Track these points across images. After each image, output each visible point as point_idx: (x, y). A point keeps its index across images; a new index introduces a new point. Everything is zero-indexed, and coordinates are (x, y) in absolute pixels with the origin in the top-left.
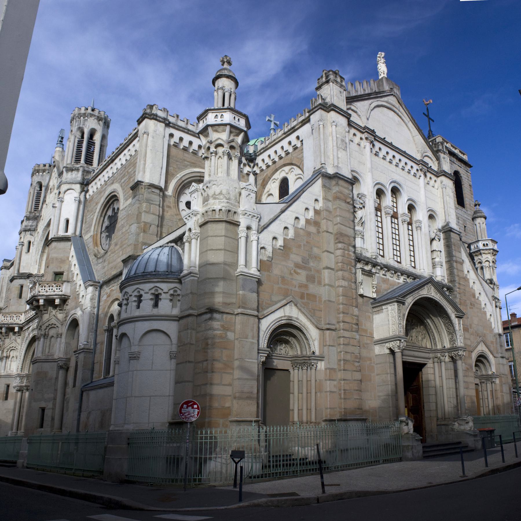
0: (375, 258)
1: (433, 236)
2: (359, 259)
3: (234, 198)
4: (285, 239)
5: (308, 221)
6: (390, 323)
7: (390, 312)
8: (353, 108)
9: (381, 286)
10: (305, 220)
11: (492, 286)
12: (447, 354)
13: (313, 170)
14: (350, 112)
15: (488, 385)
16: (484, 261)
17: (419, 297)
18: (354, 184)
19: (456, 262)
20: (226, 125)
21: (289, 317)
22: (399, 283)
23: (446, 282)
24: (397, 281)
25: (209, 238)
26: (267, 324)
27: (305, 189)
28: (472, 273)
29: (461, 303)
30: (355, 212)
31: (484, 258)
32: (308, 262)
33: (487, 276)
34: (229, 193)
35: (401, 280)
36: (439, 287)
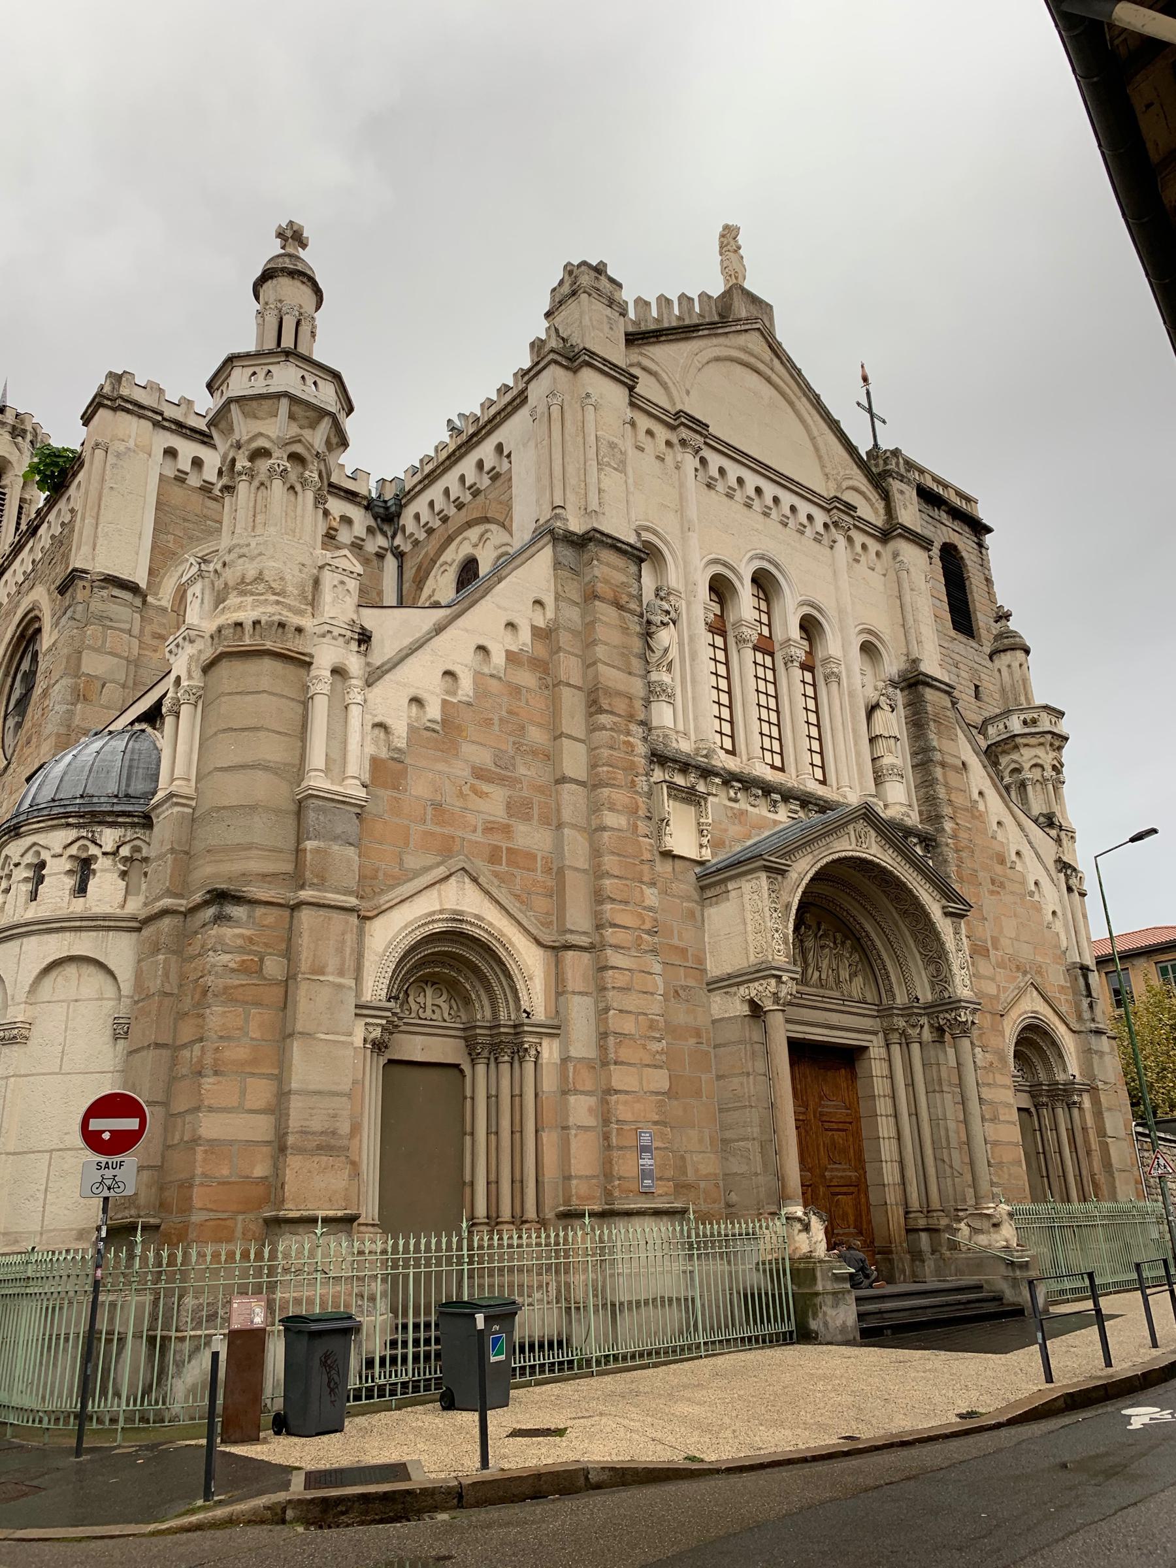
0: (706, 756)
1: (873, 696)
2: (659, 758)
3: (296, 592)
4: (445, 702)
5: (511, 657)
6: (749, 928)
7: (747, 897)
8: (646, 362)
9: (726, 830)
11: (1053, 833)
12: (924, 1020)
14: (635, 371)
15: (1060, 1111)
16: (1027, 766)
17: (830, 858)
18: (642, 561)
19: (943, 765)
20: (278, 396)
21: (455, 912)
22: (775, 822)
23: (913, 819)
24: (771, 816)
25: (224, 699)
26: (391, 933)
28: (992, 796)
31: (1026, 756)
32: (514, 765)
33: (1037, 808)
34: (282, 579)
35: (782, 815)
36: (893, 833)
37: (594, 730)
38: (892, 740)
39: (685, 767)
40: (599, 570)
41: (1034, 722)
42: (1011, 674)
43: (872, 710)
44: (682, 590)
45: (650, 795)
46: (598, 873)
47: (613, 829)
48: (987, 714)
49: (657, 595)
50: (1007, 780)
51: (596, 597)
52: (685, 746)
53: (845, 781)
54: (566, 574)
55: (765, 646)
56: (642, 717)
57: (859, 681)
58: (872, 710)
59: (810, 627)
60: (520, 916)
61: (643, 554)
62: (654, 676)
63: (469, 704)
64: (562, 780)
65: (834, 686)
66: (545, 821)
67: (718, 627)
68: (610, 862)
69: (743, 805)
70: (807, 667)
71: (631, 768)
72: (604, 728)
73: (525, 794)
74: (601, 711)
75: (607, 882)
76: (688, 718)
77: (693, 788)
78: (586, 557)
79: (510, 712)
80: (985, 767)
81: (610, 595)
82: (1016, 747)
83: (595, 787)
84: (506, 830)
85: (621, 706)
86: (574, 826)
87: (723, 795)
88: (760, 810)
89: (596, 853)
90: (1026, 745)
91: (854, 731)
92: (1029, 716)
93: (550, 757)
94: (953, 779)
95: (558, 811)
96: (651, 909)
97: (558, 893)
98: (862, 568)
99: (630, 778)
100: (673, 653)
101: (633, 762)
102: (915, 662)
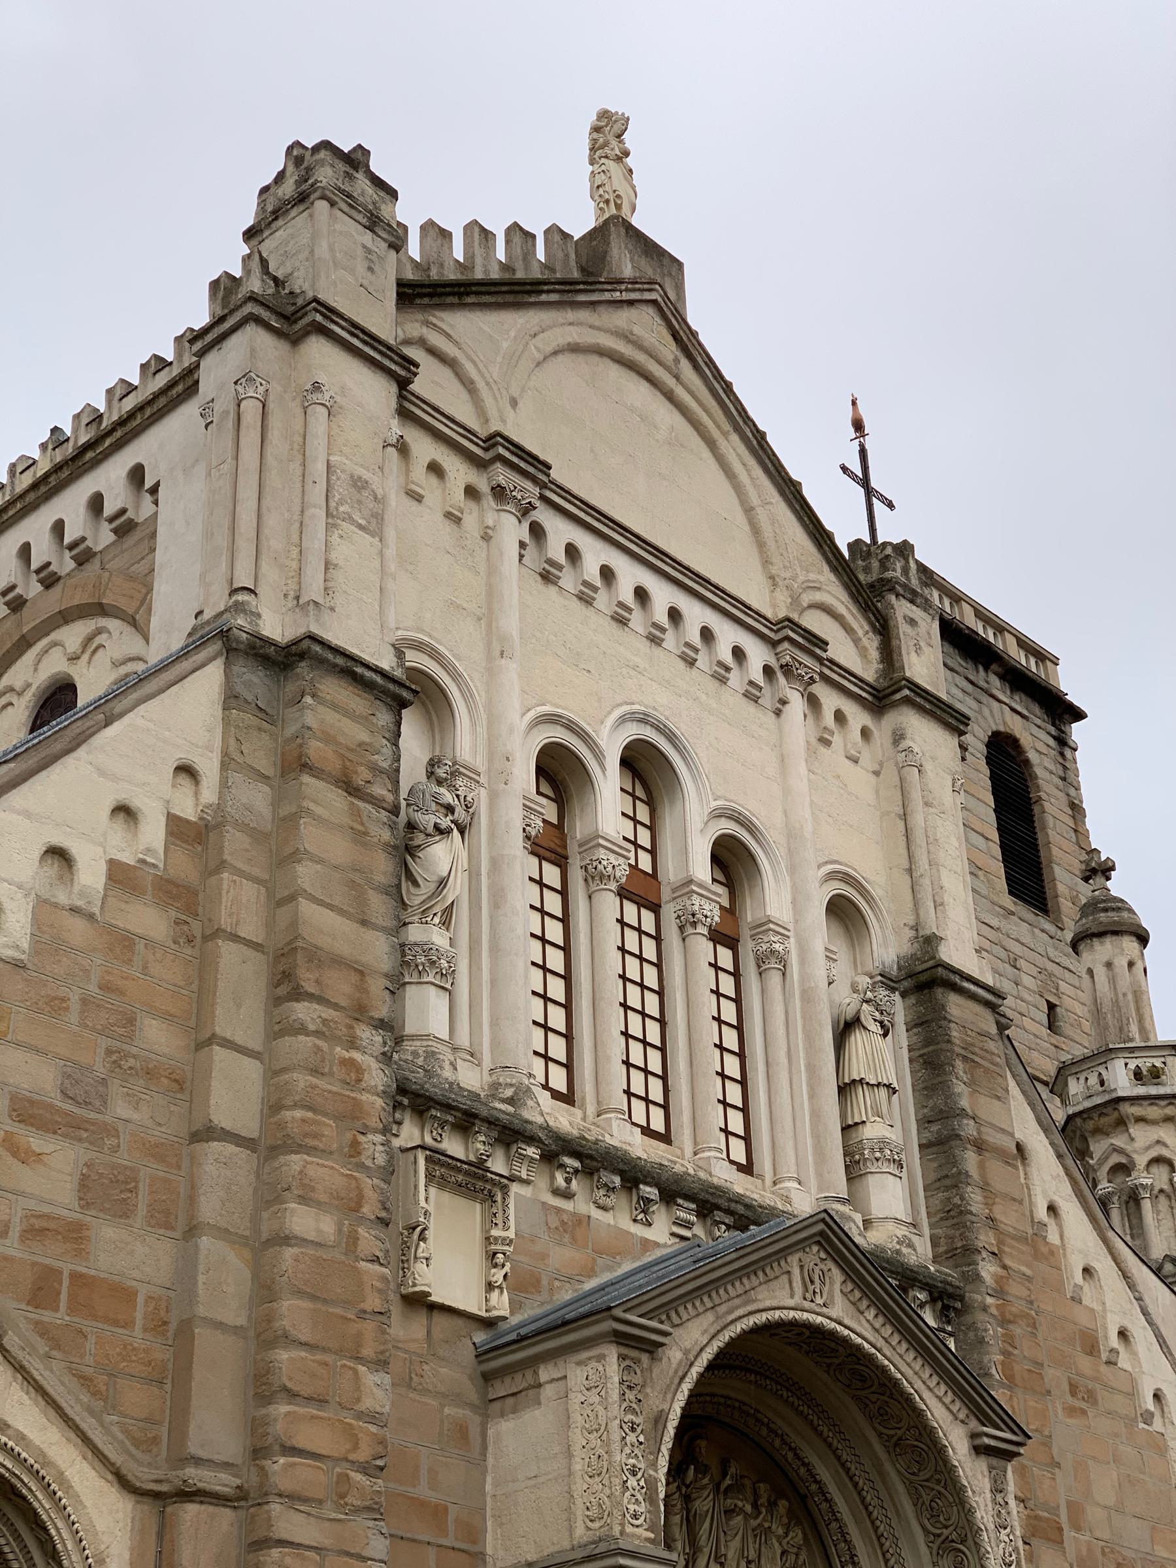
0: (510, 1101)
1: (849, 1003)
8: (435, 339)
10: (103, 868)
13: (193, 622)
16: (1141, 1161)
18: (404, 704)
19: (980, 1146)
23: (920, 1253)
24: (638, 1230)
27: (118, 707)
28: (1073, 1213)
29: (1010, 1378)
30: (411, 850)
35: (660, 1231)
37: (281, 1033)
38: (883, 1092)
39: (466, 1119)
40: (315, 715)
41: (1156, 1074)
42: (1113, 981)
43: (845, 1028)
44: (481, 768)
45: (388, 1173)
46: (265, 1335)
47: (303, 1242)
48: (1066, 1057)
49: (430, 774)
50: (1104, 1186)
51: (305, 766)
52: (470, 1078)
53: (789, 1168)
54: (249, 718)
55: (642, 891)
56: (382, 1011)
57: (822, 972)
58: (845, 1028)
59: (732, 860)
60: (88, 1424)
61: (407, 692)
62: (415, 933)
63: (18, 965)
64: (207, 1133)
65: (775, 978)
66: (161, 1219)
67: (551, 846)
68: (293, 1314)
69: (582, 1205)
70: (724, 937)
71: (351, 1116)
72: (302, 1030)
73: (123, 1158)
74: (298, 995)
75: (283, 1356)
76: (482, 1019)
77: (480, 1164)
78: (291, 688)
79: (105, 987)
80: (1060, 1156)
81: (334, 765)
82: (1121, 1123)
83: (275, 1151)
84: (75, 1234)
85: (340, 987)
86: (223, 1233)
87: (542, 1183)
88: (617, 1218)
89: (265, 1291)
90: (1140, 1120)
91: (811, 1069)
92: (1145, 1063)
93: (185, 1084)
94: (997, 1172)
95: (192, 1200)
96: (372, 1417)
97: (175, 1378)
98: (834, 756)
99: (349, 1136)
100: (457, 889)
101: (357, 1104)
102: (930, 942)
